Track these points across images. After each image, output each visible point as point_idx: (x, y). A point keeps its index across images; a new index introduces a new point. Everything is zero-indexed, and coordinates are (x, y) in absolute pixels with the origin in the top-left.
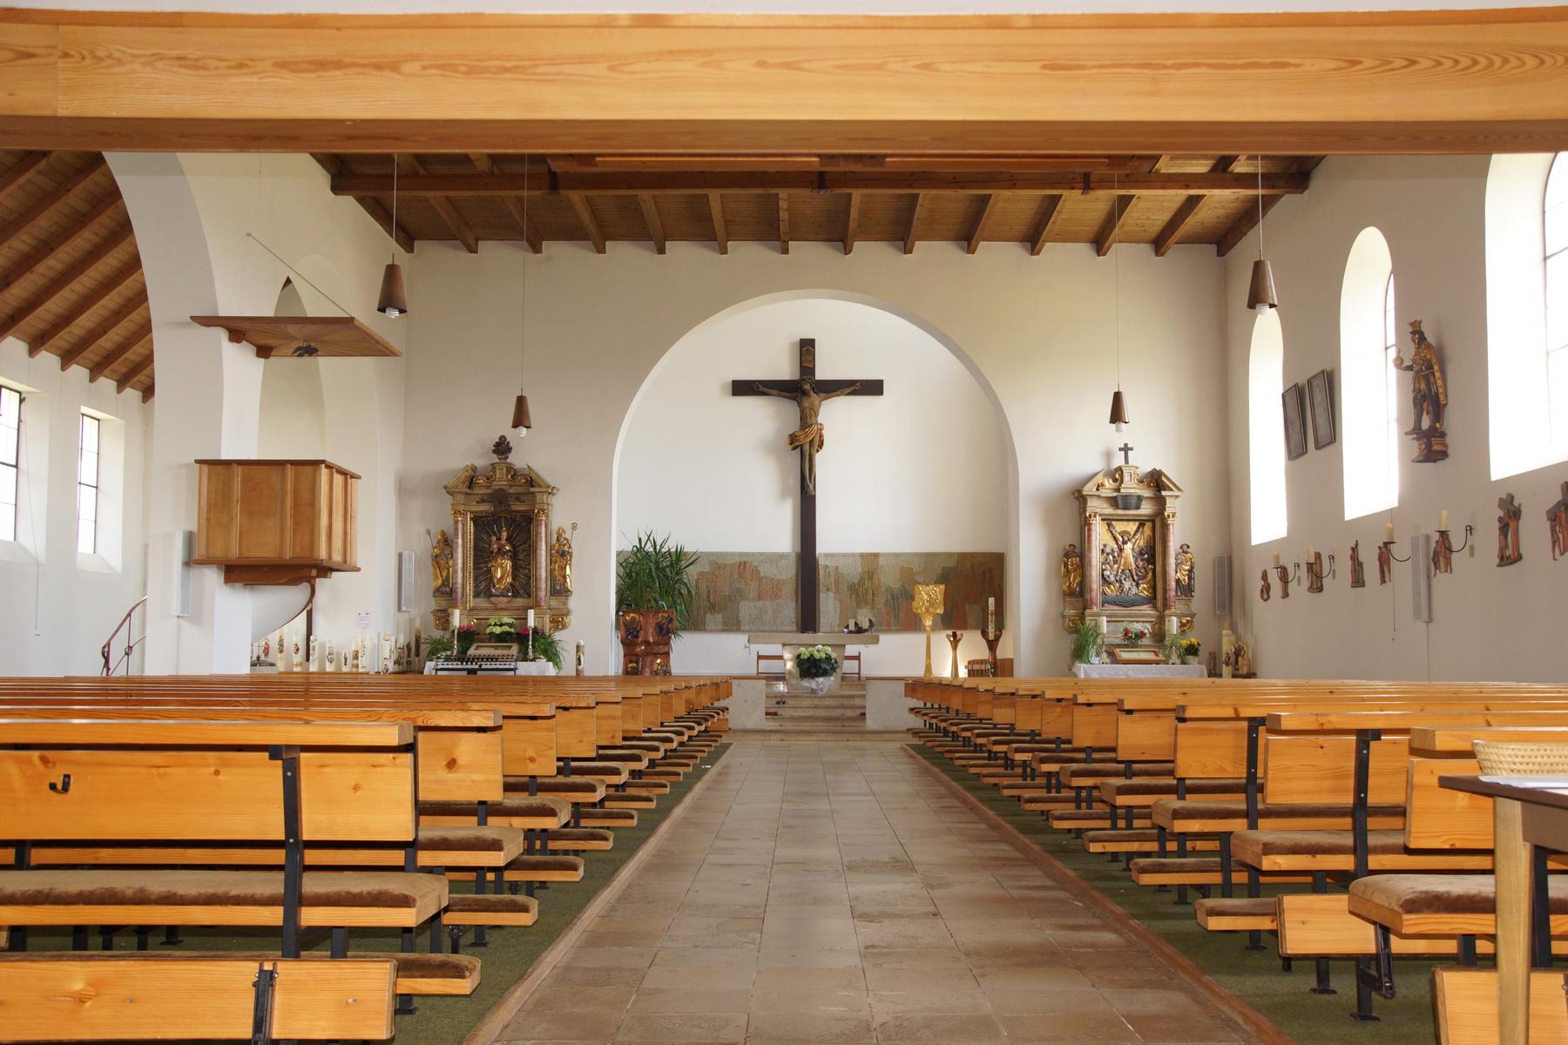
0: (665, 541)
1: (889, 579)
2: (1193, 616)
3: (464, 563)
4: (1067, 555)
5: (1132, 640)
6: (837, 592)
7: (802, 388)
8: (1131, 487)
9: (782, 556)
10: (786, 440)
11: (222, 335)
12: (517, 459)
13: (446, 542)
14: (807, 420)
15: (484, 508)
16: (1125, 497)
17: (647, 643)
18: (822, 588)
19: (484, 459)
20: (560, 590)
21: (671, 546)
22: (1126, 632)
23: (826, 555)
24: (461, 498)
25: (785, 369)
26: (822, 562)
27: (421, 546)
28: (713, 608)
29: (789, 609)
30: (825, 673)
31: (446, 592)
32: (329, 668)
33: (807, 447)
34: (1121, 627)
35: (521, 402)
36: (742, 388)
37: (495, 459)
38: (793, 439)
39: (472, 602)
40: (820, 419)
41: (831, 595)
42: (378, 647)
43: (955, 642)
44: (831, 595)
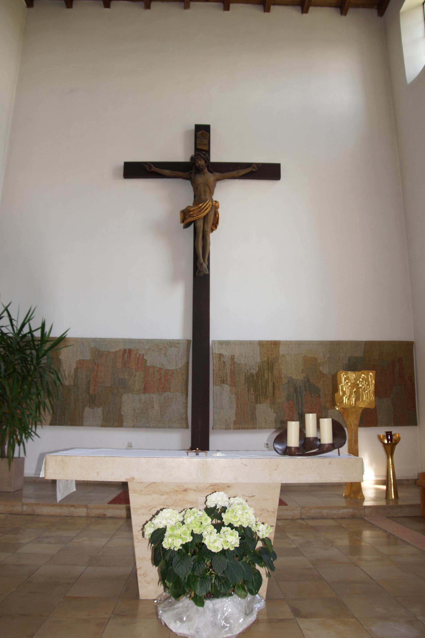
1: (291, 370)
6: (233, 384)
9: (172, 344)
10: (178, 217)
14: (202, 195)
23: (221, 343)
25: (180, 151)
28: (93, 401)
29: (182, 403)
33: (200, 224)
36: (134, 170)
41: (226, 387)
43: (390, 446)
44: (226, 387)
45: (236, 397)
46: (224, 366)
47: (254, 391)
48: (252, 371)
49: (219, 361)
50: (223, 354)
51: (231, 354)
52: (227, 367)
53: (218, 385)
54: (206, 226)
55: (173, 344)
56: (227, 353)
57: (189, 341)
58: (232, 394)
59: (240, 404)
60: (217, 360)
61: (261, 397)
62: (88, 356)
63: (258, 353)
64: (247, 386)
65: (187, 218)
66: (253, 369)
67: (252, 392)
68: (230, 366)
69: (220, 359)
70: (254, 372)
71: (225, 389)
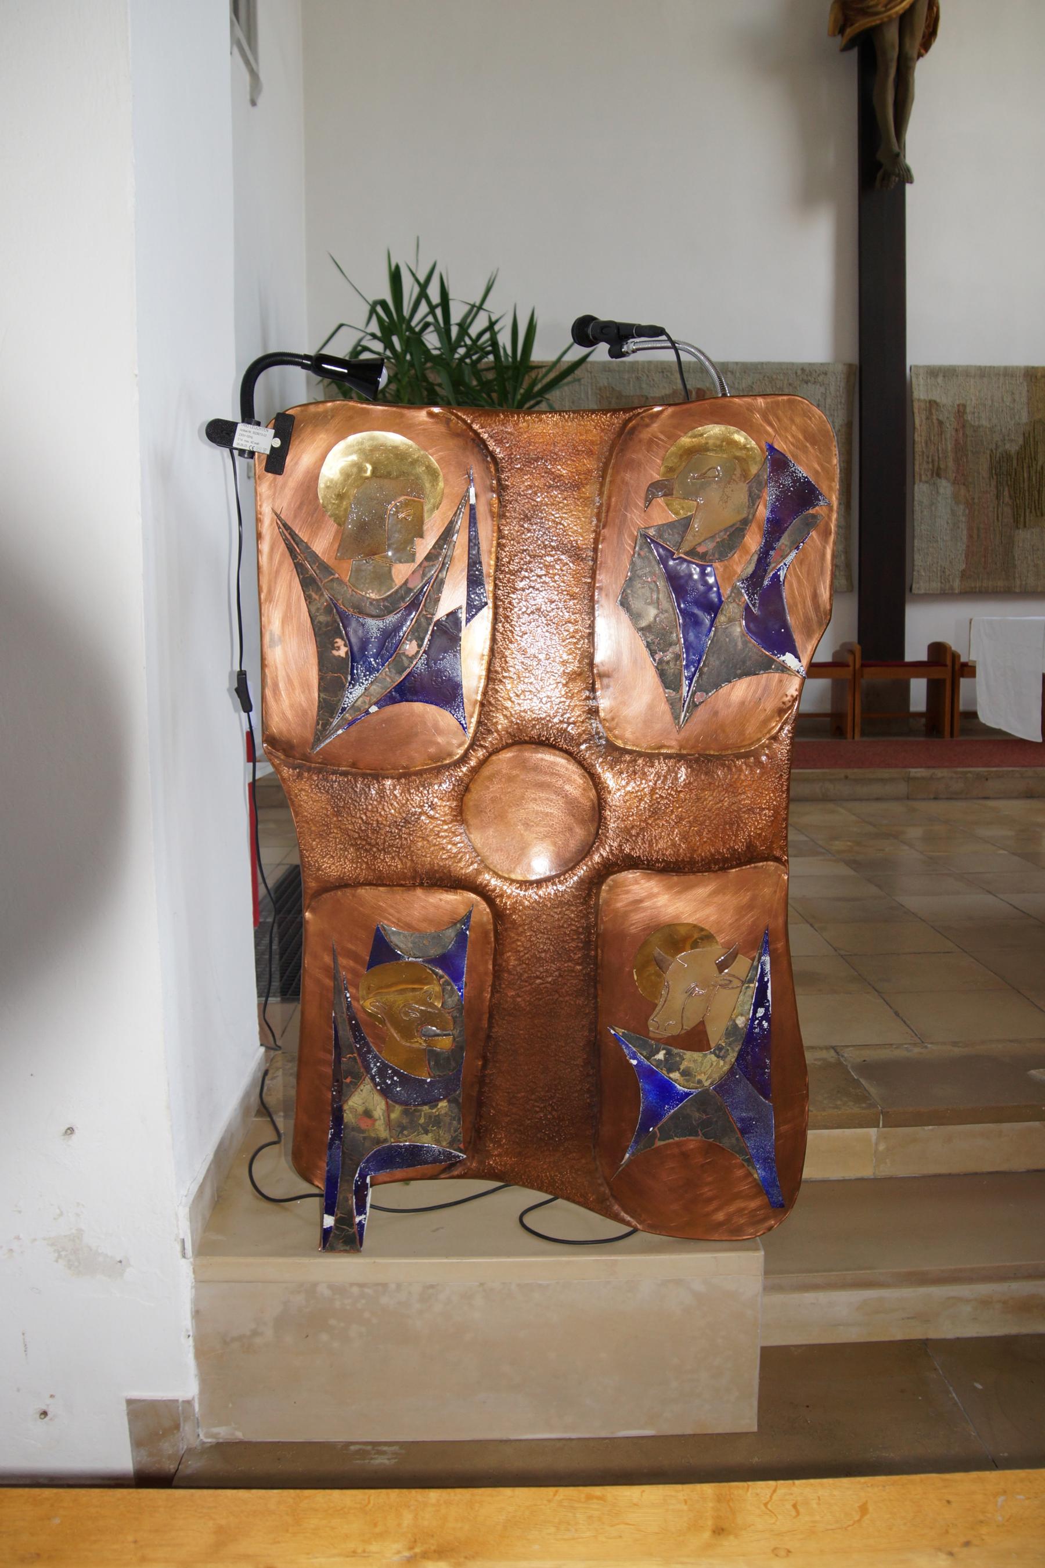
0: (476, 309)
6: (962, 480)
9: (807, 374)
18: (919, 466)
23: (933, 372)
26: (920, 391)
33: (892, 34)
41: (945, 487)
44: (945, 487)
45: (967, 511)
46: (941, 433)
47: (1010, 497)
48: (1007, 446)
49: (927, 418)
50: (938, 400)
51: (958, 402)
52: (948, 436)
53: (926, 482)
54: (907, 41)
55: (811, 374)
56: (946, 397)
57: (850, 366)
58: (957, 503)
59: (978, 529)
60: (924, 417)
61: (1028, 511)
63: (1024, 400)
64: (993, 483)
66: (1011, 441)
67: (1007, 499)
68: (954, 433)
69: (931, 413)
70: (1013, 448)
71: (942, 491)
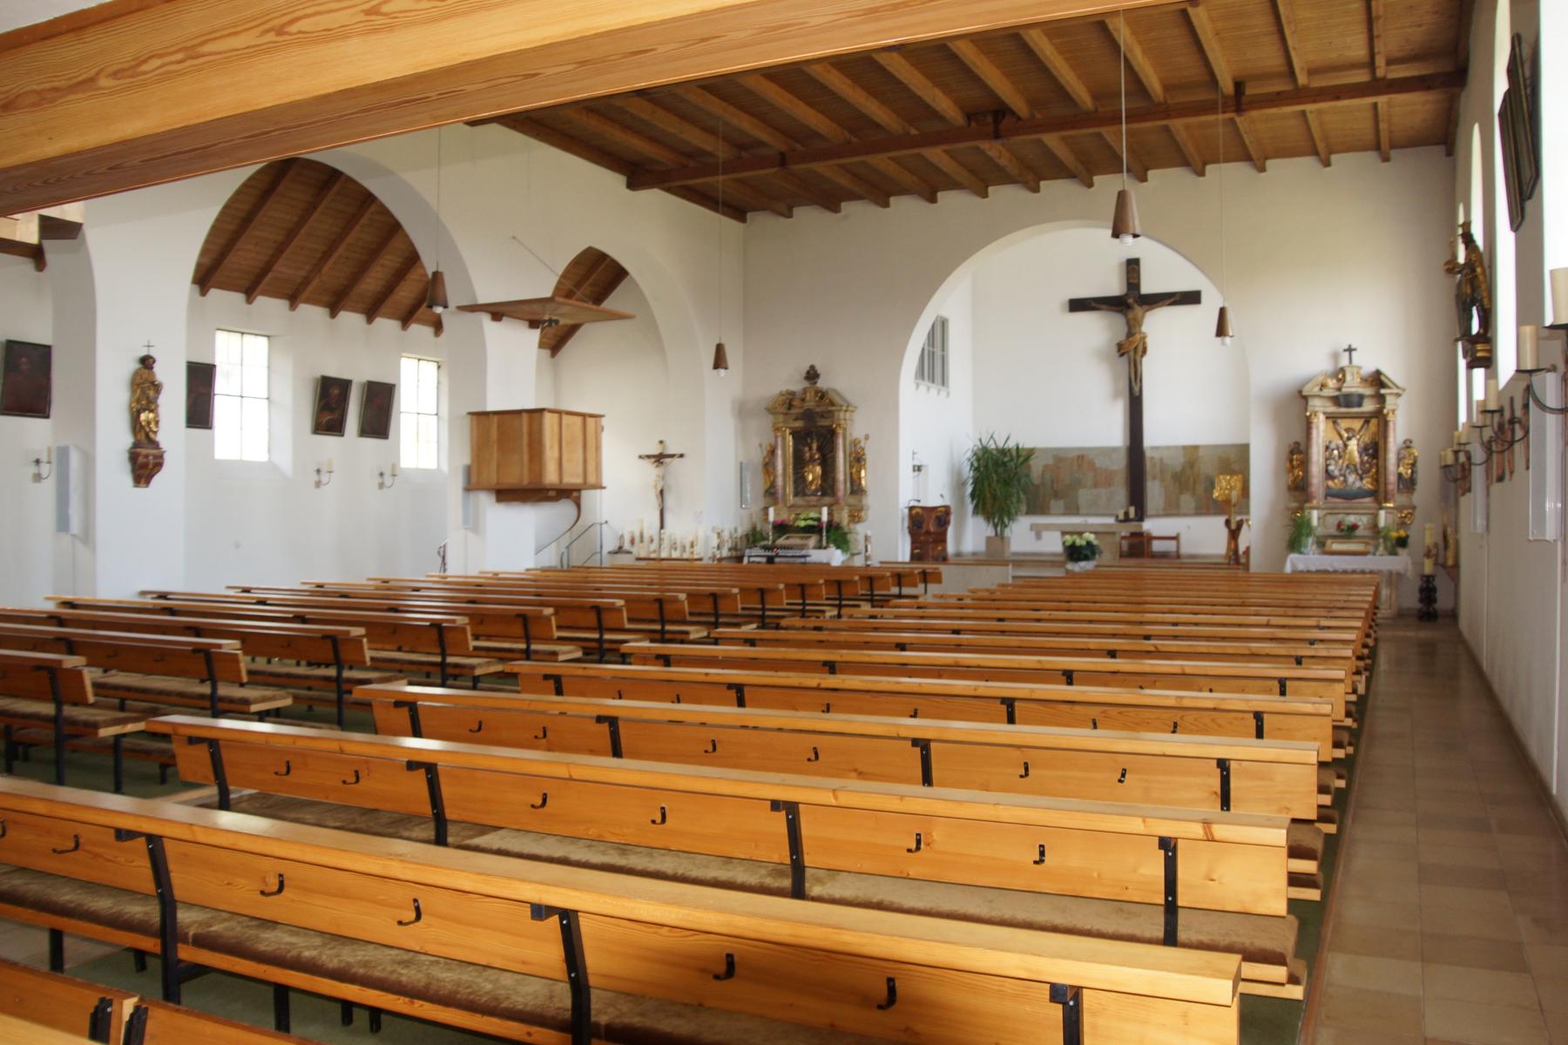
2: (1414, 508)
3: (785, 469)
4: (1292, 453)
5: (1348, 532)
6: (1163, 480)
7: (1130, 302)
8: (1353, 385)
10: (1115, 349)
11: (486, 319)
12: (821, 384)
13: (773, 452)
14: (1133, 328)
15: (799, 424)
16: (1347, 396)
17: (928, 532)
18: (1149, 476)
19: (798, 385)
20: (857, 489)
21: (1011, 444)
22: (1339, 525)
23: (1153, 448)
24: (781, 418)
25: (1114, 286)
26: (1148, 454)
27: (757, 456)
28: (1056, 495)
30: (1086, 558)
31: (771, 493)
32: (675, 555)
34: (1332, 520)
35: (720, 349)
36: (1077, 305)
37: (806, 384)
38: (1120, 346)
39: (791, 499)
40: (1144, 329)
41: (1157, 483)
42: (707, 539)
44: (1157, 483)
56: (1157, 455)
62: (1051, 462)
65: (1121, 349)
